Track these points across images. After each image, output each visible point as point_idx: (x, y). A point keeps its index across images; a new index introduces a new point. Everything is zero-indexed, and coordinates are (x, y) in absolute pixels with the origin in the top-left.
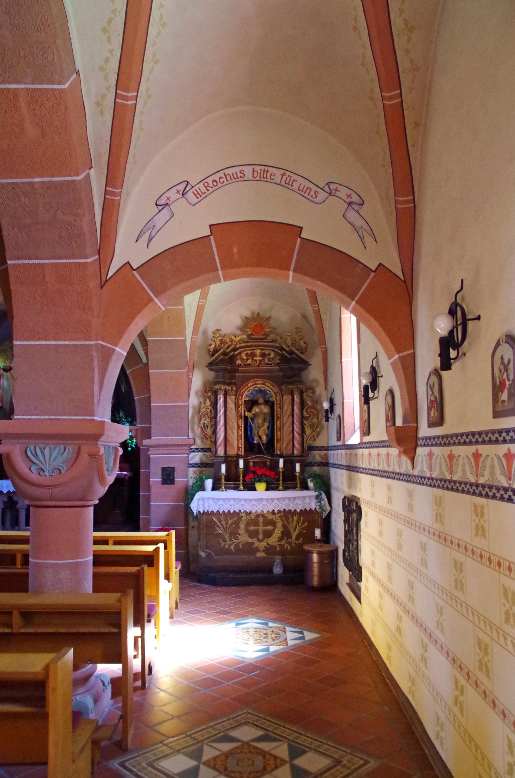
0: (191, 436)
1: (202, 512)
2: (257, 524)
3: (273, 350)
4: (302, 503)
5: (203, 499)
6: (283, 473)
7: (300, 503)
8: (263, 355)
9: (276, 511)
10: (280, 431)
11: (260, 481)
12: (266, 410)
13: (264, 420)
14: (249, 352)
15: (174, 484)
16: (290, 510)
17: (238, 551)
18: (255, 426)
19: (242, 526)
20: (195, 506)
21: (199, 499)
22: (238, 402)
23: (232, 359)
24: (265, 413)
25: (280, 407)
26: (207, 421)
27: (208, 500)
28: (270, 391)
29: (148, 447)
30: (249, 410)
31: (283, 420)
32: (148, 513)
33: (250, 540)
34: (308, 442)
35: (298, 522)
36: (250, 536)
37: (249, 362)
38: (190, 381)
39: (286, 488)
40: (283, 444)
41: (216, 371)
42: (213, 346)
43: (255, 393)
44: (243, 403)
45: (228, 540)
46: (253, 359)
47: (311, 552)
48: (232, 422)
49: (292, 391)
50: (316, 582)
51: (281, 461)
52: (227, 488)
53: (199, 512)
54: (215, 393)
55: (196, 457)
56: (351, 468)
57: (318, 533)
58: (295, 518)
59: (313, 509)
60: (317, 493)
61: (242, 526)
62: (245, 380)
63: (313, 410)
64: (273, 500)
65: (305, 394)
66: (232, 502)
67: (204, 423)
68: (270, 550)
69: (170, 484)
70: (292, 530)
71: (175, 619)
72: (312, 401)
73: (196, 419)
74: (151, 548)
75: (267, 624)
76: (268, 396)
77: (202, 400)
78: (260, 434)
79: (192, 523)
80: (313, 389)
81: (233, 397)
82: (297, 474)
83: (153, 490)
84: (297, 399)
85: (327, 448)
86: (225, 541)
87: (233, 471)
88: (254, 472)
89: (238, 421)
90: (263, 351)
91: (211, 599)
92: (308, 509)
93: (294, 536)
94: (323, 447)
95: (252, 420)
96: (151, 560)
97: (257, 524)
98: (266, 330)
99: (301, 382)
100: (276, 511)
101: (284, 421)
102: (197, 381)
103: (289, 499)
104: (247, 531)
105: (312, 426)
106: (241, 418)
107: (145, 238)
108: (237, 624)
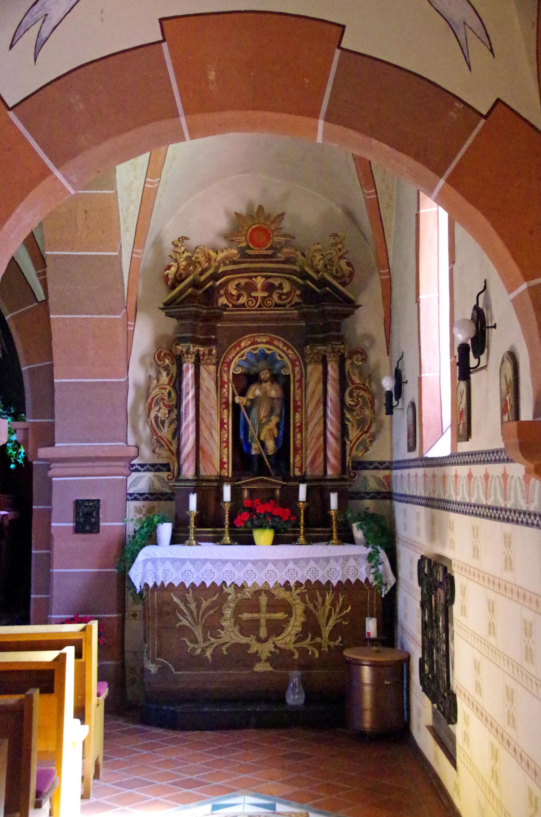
0: (131, 441)
1: (151, 585)
2: (255, 607)
3: (288, 279)
4: (342, 568)
5: (154, 561)
6: (306, 510)
7: (338, 568)
8: (269, 288)
9: (292, 583)
10: (301, 431)
11: (261, 526)
12: (274, 392)
13: (271, 412)
14: (243, 282)
15: (98, 532)
17: (219, 661)
18: (253, 424)
19: (228, 613)
20: (140, 574)
21: (146, 561)
22: (221, 376)
23: (210, 296)
24: (272, 399)
25: (300, 386)
26: (163, 413)
27: (163, 563)
28: (282, 357)
29: (49, 462)
30: (243, 393)
31: (306, 412)
32: (47, 589)
33: (244, 640)
34: (355, 453)
35: (333, 604)
36: (243, 632)
37: (243, 300)
38: (129, 336)
39: (310, 541)
40: (306, 457)
41: (179, 317)
42: (173, 269)
43: (253, 360)
44: (231, 378)
45: (200, 639)
46: (249, 296)
47: (359, 664)
48: (211, 415)
49: (324, 357)
50: (367, 721)
51: (303, 489)
52: (199, 540)
53: (146, 585)
54: (179, 361)
55: (141, 482)
56: (435, 503)
57: (371, 626)
58: (329, 598)
59: (363, 580)
60: (370, 550)
61: (228, 613)
62: (235, 336)
63: (362, 393)
64: (286, 562)
65: (348, 363)
66: (208, 566)
67: (156, 417)
68: (279, 658)
69: (90, 532)
70: (322, 621)
71: (92, 799)
72: (361, 375)
73: (141, 408)
74: (48, 656)
75: (272, 807)
76: (278, 366)
77: (153, 373)
78: (262, 438)
79: (132, 607)
80: (363, 354)
81: (212, 368)
82: (333, 513)
83: (58, 544)
84: (332, 371)
85: (389, 466)
86: (195, 641)
87: (212, 507)
88: (251, 510)
89: (221, 414)
90: (271, 280)
91: (164, 758)
92: (353, 580)
93: (326, 631)
94: (381, 463)
95: (249, 410)
96: (47, 680)
97: (255, 607)
98: (276, 239)
99: (341, 339)
100: (292, 583)
101: (309, 412)
102: (144, 335)
103: (317, 560)
104: (237, 621)
105: (361, 423)
106: (227, 408)
107: (29, 40)
108: (215, 808)
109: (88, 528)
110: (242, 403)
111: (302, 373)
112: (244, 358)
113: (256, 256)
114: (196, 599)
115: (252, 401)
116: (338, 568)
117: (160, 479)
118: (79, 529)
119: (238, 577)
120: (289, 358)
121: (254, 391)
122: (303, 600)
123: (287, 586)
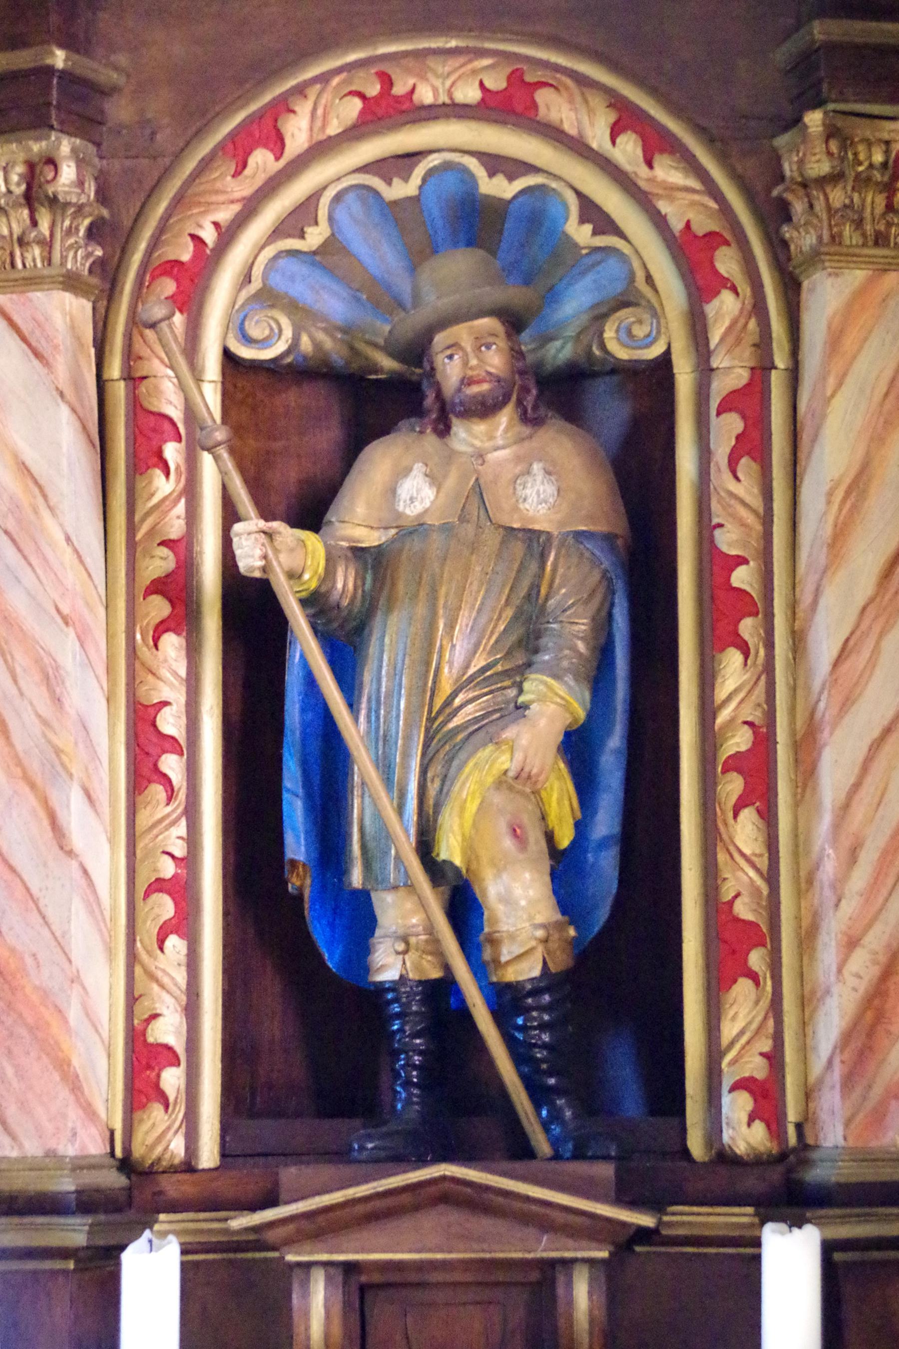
10: (761, 795)
12: (545, 483)
13: (527, 640)
18: (382, 741)
22: (133, 379)
24: (535, 542)
25: (752, 445)
28: (603, 223)
30: (310, 510)
31: (798, 641)
40: (808, 1002)
43: (378, 253)
44: (211, 396)
48: (51, 679)
76: (575, 302)
78: (450, 849)
89: (136, 668)
95: (345, 646)
101: (824, 647)
106: (184, 617)
110: (294, 576)
111: (764, 344)
112: (315, 236)
115: (374, 562)
120: (659, 222)
121: (392, 491)
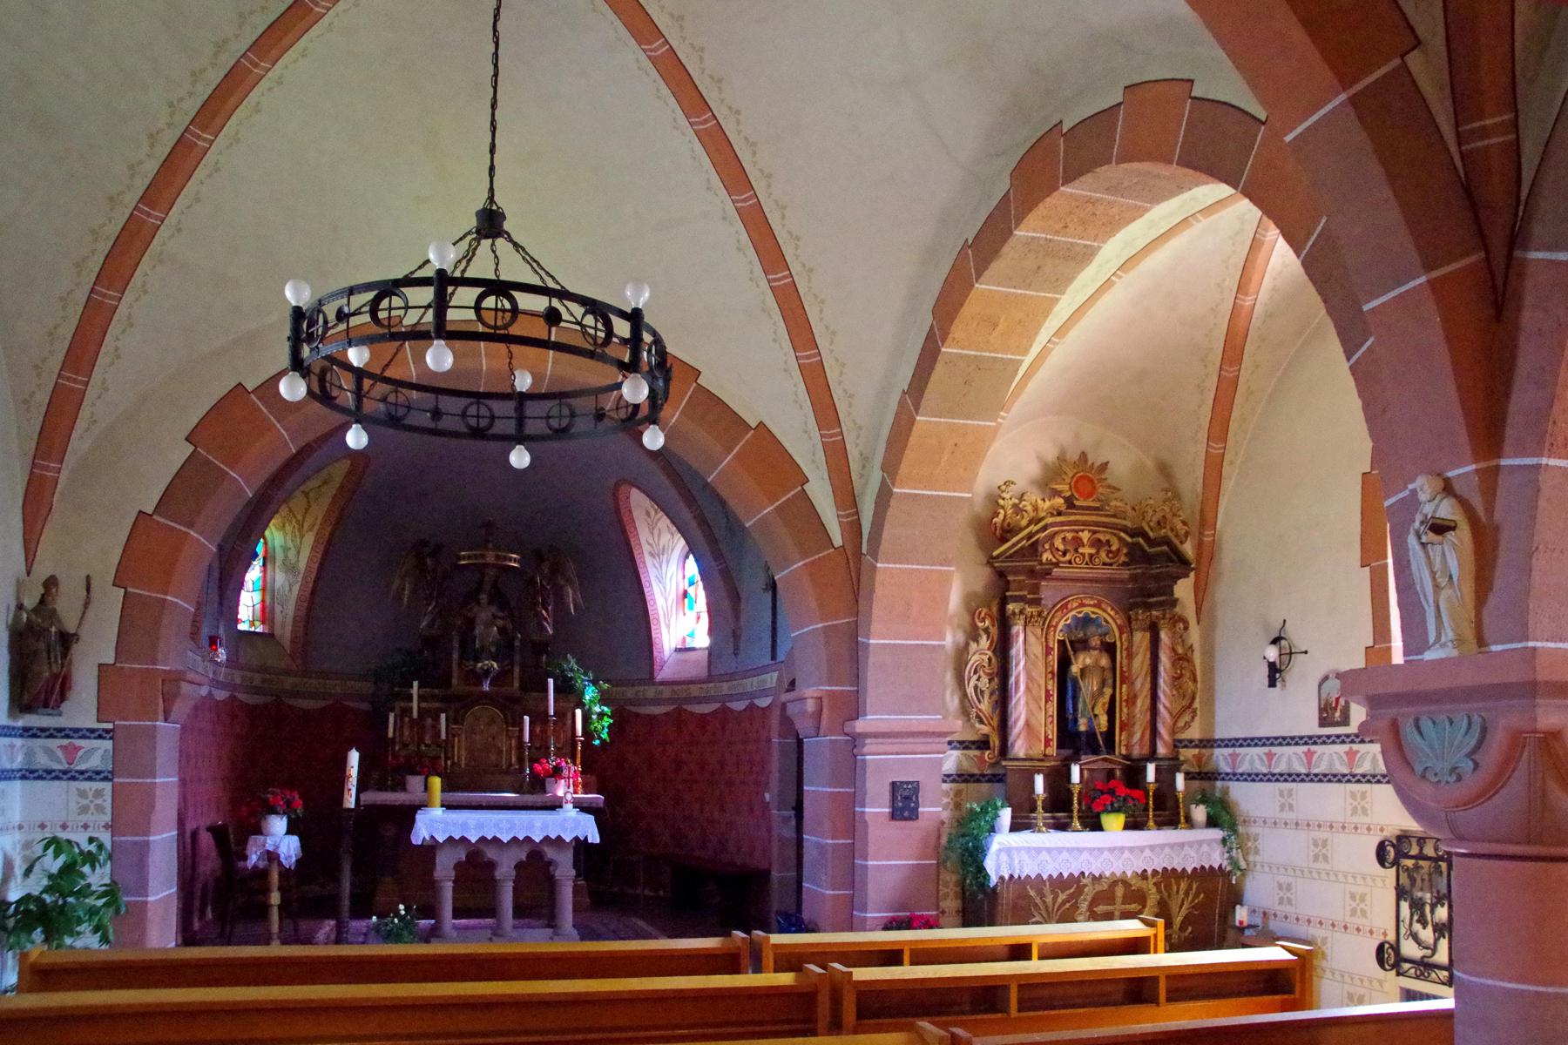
4: (1197, 851)
7: (1193, 854)
12: (1104, 661)
16: (1174, 870)
21: (1000, 851)
35: (1187, 894)
53: (1002, 878)
55: (952, 761)
58: (1183, 886)
64: (1142, 849)
66: (1065, 855)
67: (976, 687)
83: (874, 833)
103: (1172, 846)
109: (906, 814)
113: (1088, 508)
114: (1053, 892)
116: (1193, 854)
117: (968, 758)
118: (895, 815)
119: (1094, 866)
122: (1159, 891)
123: (1144, 875)
